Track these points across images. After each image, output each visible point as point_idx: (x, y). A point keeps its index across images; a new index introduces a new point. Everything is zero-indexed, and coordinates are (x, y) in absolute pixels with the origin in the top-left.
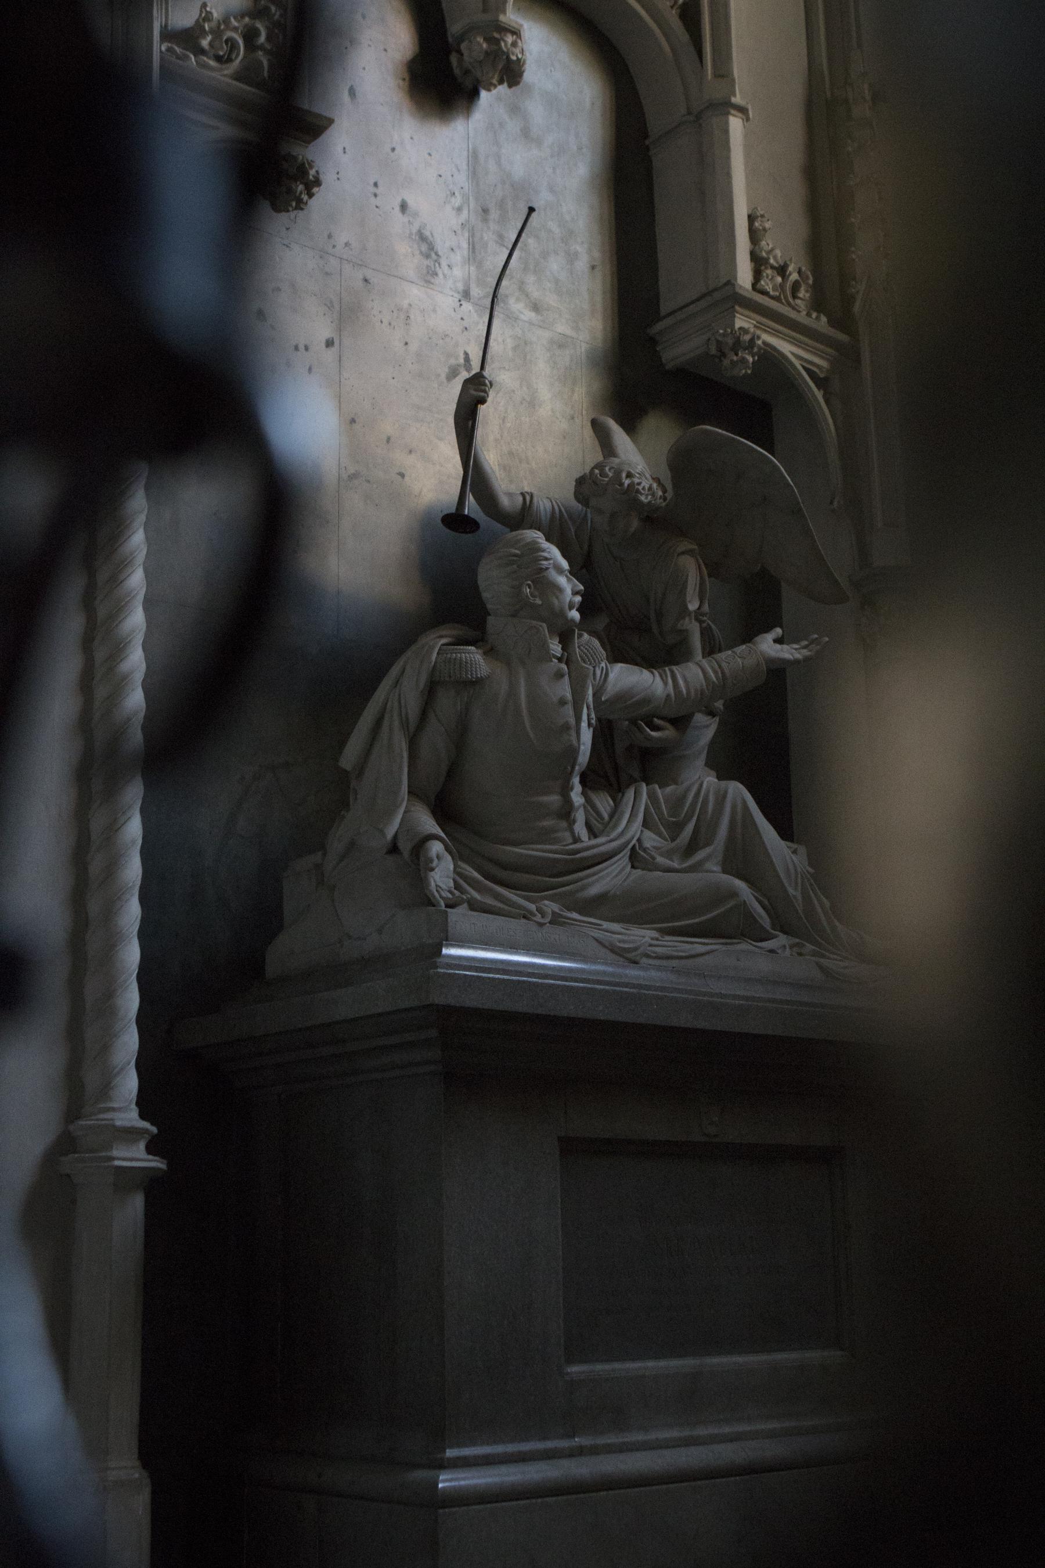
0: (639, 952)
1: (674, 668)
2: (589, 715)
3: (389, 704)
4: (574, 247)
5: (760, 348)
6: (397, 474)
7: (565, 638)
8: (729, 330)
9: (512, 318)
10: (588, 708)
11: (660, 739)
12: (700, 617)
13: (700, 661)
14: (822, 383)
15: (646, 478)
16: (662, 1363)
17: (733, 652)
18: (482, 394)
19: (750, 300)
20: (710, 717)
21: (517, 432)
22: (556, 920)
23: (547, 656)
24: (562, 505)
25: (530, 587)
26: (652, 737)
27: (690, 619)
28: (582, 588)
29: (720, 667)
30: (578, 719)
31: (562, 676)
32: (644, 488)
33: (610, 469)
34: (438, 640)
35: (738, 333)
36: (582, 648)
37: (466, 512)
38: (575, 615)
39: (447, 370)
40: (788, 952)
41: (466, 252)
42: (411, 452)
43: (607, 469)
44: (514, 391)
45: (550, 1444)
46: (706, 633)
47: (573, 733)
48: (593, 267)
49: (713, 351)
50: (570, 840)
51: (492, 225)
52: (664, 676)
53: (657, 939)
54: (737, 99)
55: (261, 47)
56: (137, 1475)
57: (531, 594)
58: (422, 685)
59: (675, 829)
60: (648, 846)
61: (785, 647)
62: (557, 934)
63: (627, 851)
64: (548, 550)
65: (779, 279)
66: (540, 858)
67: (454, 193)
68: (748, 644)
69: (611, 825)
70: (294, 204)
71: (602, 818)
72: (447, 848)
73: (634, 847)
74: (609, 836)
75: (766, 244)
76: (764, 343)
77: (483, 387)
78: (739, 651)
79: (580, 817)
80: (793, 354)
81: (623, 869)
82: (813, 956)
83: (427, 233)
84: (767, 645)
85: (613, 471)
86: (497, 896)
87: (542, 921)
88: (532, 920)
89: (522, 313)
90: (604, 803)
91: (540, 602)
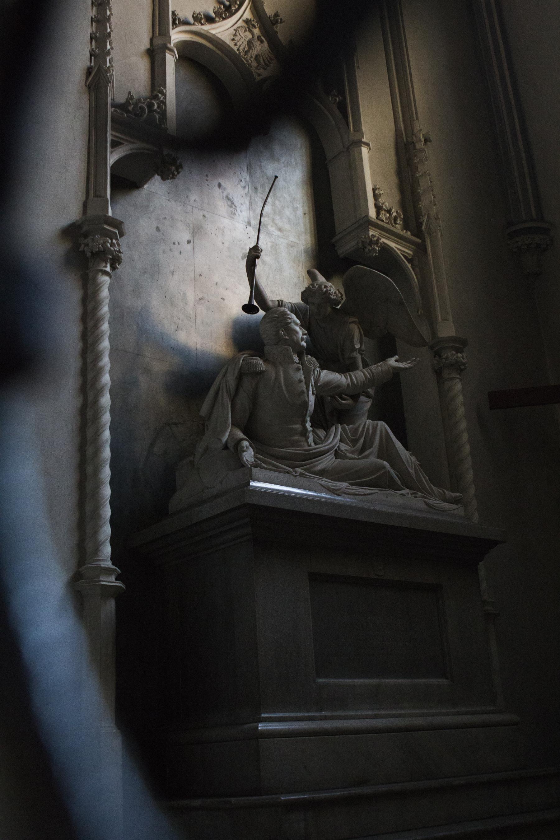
0: (341, 491)
1: (350, 373)
2: (312, 389)
4: (296, 205)
5: (381, 244)
7: (300, 356)
8: (367, 236)
9: (269, 234)
10: (312, 386)
11: (346, 404)
14: (409, 261)
16: (362, 680)
17: (377, 365)
18: (258, 254)
19: (375, 223)
20: (368, 398)
22: (301, 475)
23: (293, 362)
25: (282, 330)
29: (371, 372)
30: (308, 390)
31: (300, 370)
32: (332, 292)
33: (317, 285)
35: (371, 237)
38: (304, 344)
39: (242, 255)
40: (410, 495)
41: (248, 206)
42: (227, 289)
43: (315, 284)
45: (310, 714)
46: (363, 361)
47: (306, 395)
48: (305, 214)
49: (360, 246)
51: (259, 194)
54: (364, 140)
55: (155, 111)
56: (115, 731)
58: (236, 374)
59: (354, 442)
60: (343, 449)
62: (302, 480)
65: (388, 215)
67: (242, 181)
70: (171, 176)
72: (251, 445)
73: (336, 450)
75: (381, 200)
76: (382, 242)
77: (258, 251)
79: (311, 435)
80: (396, 247)
81: (332, 458)
82: (422, 498)
83: (230, 197)
84: (392, 362)
85: (318, 285)
86: (274, 466)
87: (295, 474)
88: (292, 475)
89: (274, 232)
90: (321, 433)
91: (288, 338)
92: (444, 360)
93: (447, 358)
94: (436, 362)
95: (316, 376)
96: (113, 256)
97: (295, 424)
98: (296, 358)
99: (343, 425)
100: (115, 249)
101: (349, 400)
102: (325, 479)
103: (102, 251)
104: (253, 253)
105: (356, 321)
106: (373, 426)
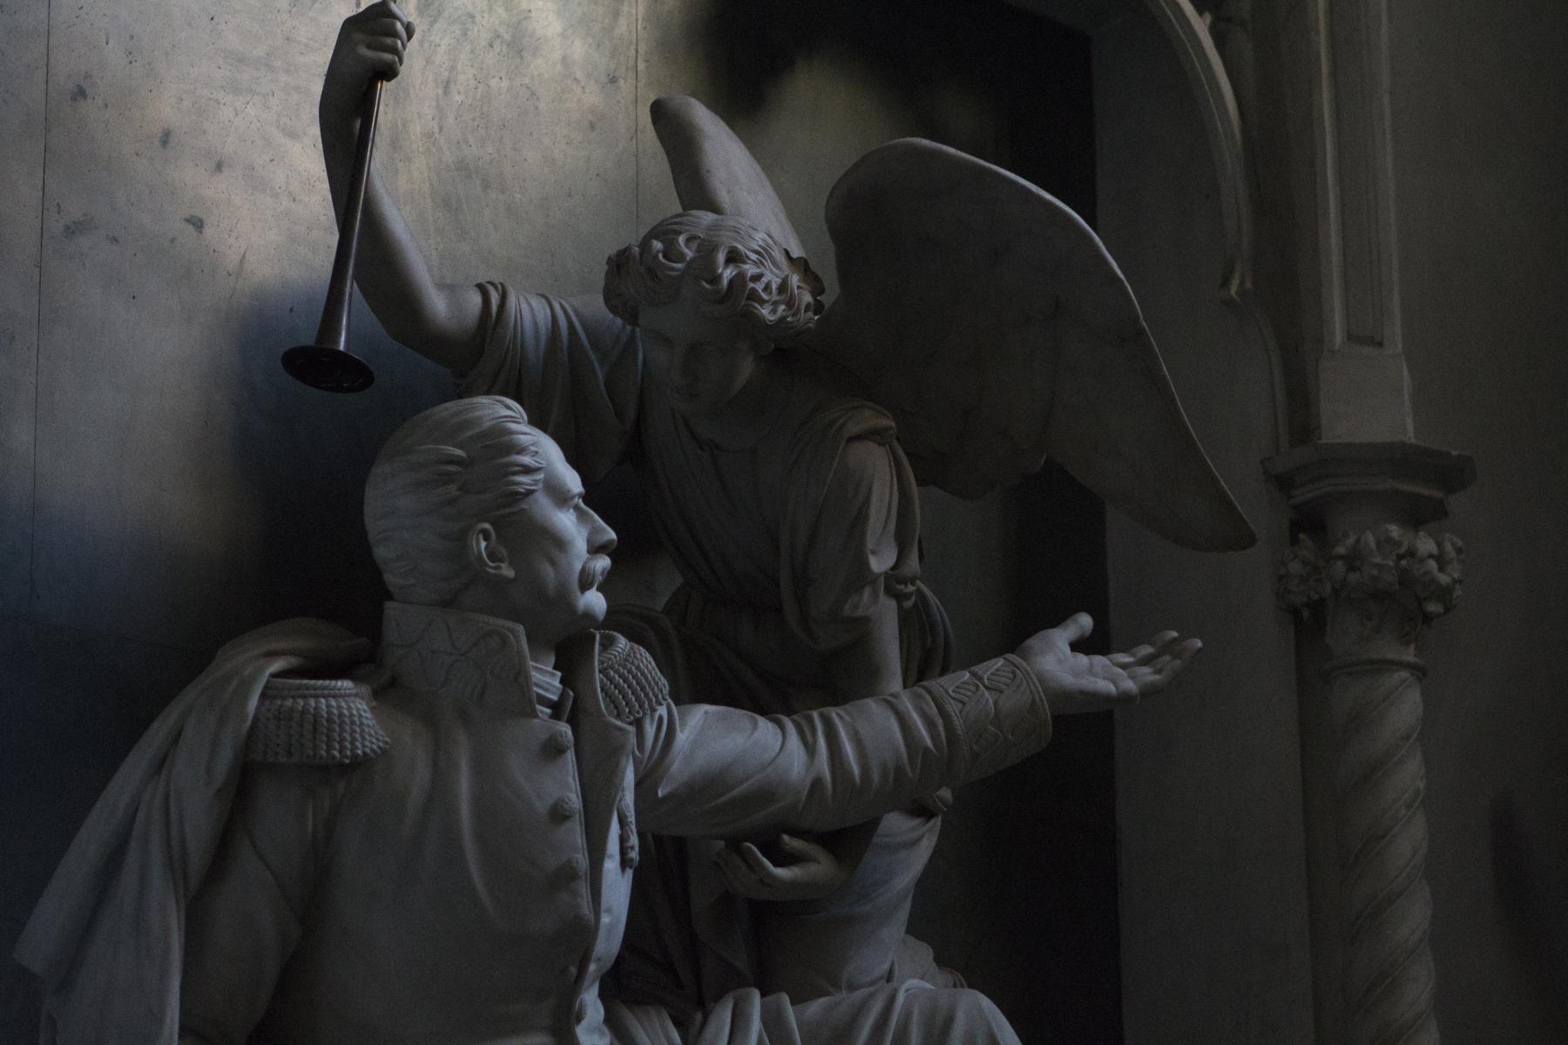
1: (833, 713)
2: (623, 840)
3: (141, 816)
6: (187, 220)
10: (623, 822)
11: (794, 884)
12: (901, 587)
13: (894, 696)
15: (775, 263)
18: (388, 57)
20: (918, 821)
21: (478, 114)
25: (487, 538)
28: (612, 535)
32: (767, 288)
33: (688, 241)
36: (612, 673)
37: (342, 347)
38: (595, 601)
42: (219, 167)
43: (681, 239)
44: (472, 17)
47: (584, 889)
52: (806, 729)
61: (1099, 660)
64: (533, 448)
68: (1010, 656)
77: (389, 41)
78: (988, 673)
85: (694, 245)
93: (1354, 560)
94: (1295, 567)
95: (647, 754)
98: (547, 679)
99: (770, 999)
101: (814, 860)
104: (364, 51)
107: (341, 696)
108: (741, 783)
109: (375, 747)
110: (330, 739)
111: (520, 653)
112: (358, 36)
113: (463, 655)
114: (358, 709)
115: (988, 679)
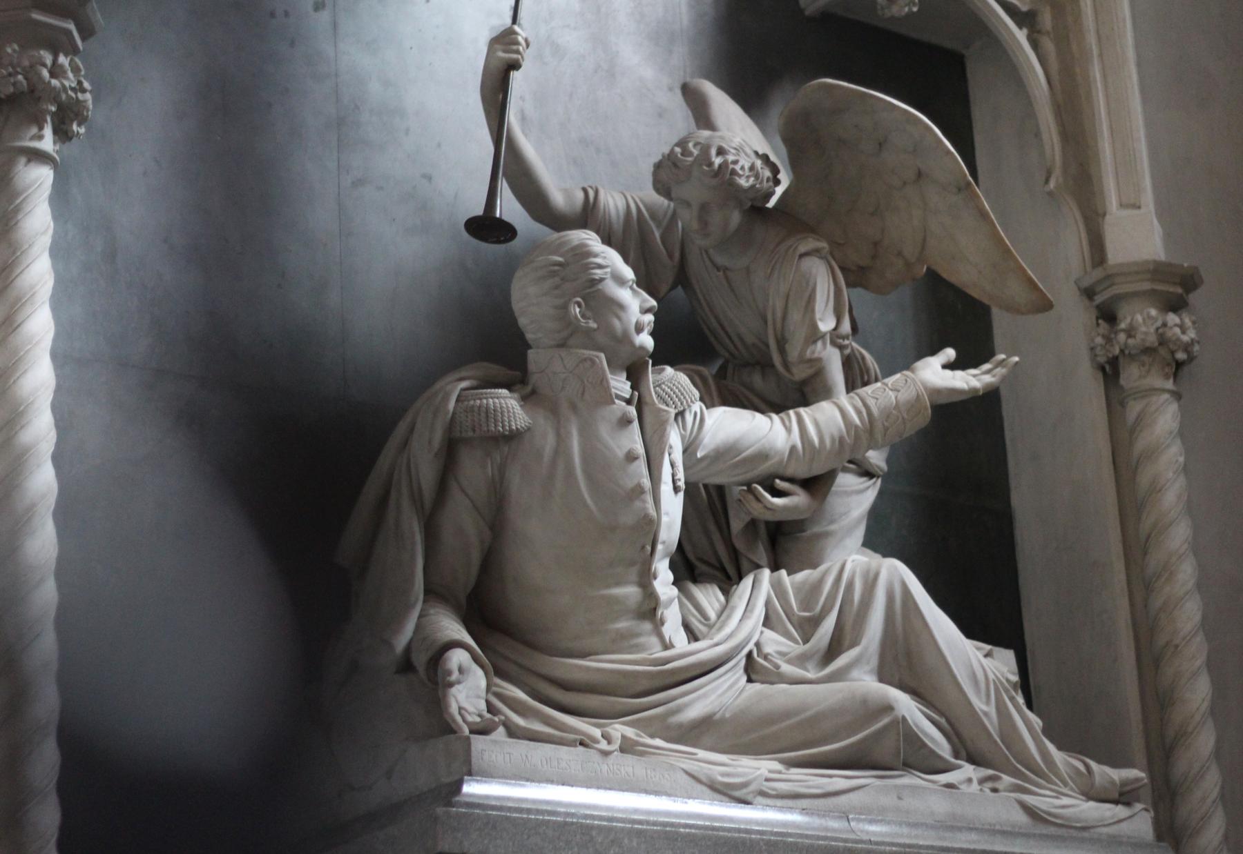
0: (752, 787)
1: (802, 410)
7: (635, 374)
10: (672, 465)
11: (785, 508)
12: (841, 341)
15: (746, 154)
17: (884, 384)
20: (864, 479)
22: (628, 747)
23: (607, 398)
24: (641, 200)
25: (580, 306)
26: (777, 506)
27: (824, 344)
28: (654, 303)
29: (865, 404)
31: (630, 422)
33: (695, 145)
34: (456, 383)
38: (646, 341)
40: (975, 786)
43: (691, 145)
46: (849, 363)
47: (649, 499)
50: (658, 647)
53: (780, 772)
57: (583, 316)
59: (807, 627)
62: (629, 765)
63: (741, 659)
64: (603, 255)
66: (612, 671)
68: (906, 372)
69: (718, 625)
71: (706, 617)
73: (749, 655)
74: (712, 639)
77: (515, 47)
85: (699, 147)
86: (548, 721)
88: (596, 749)
90: (709, 597)
92: (1122, 337)
94: (1099, 340)
96: (61, 107)
97: (618, 584)
99: (776, 574)
100: (67, 83)
101: (798, 495)
102: (702, 754)
103: (22, 93)
104: (501, 54)
105: (824, 248)
106: (866, 575)
107: (501, 397)
108: (748, 449)
109: (523, 426)
110: (496, 421)
111: (604, 371)
112: (498, 46)
113: (571, 372)
114: (511, 404)
115: (892, 385)
